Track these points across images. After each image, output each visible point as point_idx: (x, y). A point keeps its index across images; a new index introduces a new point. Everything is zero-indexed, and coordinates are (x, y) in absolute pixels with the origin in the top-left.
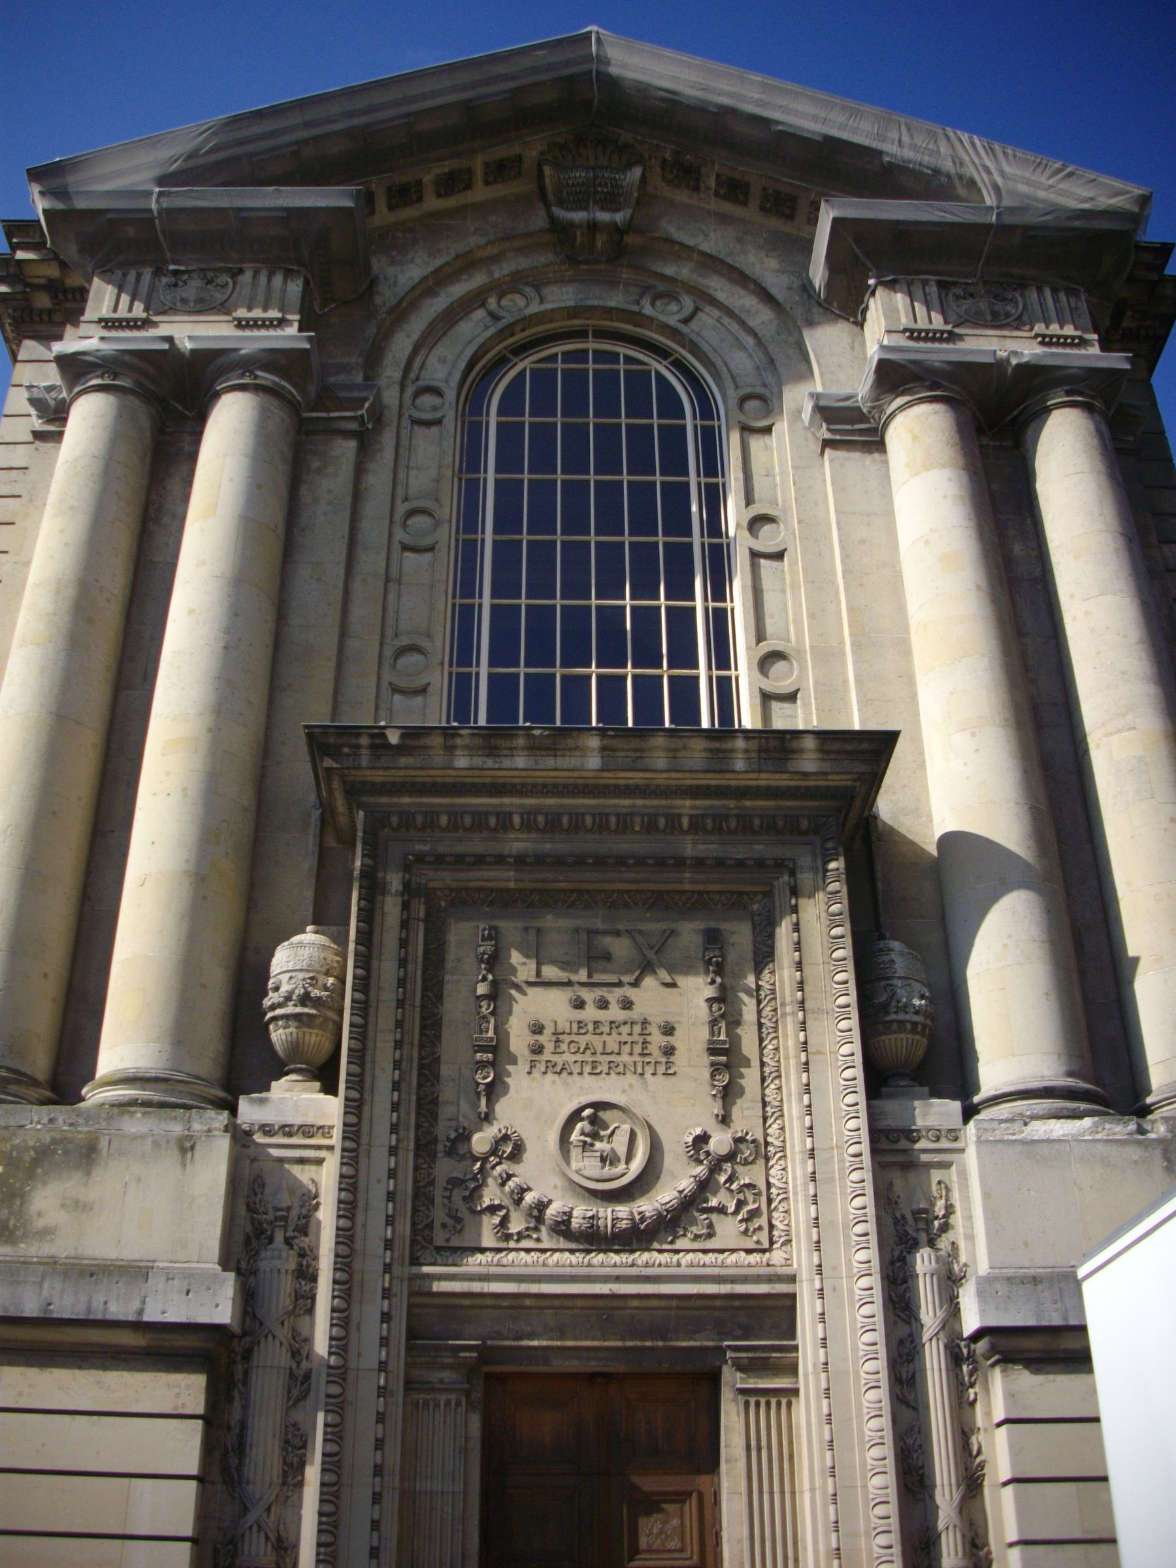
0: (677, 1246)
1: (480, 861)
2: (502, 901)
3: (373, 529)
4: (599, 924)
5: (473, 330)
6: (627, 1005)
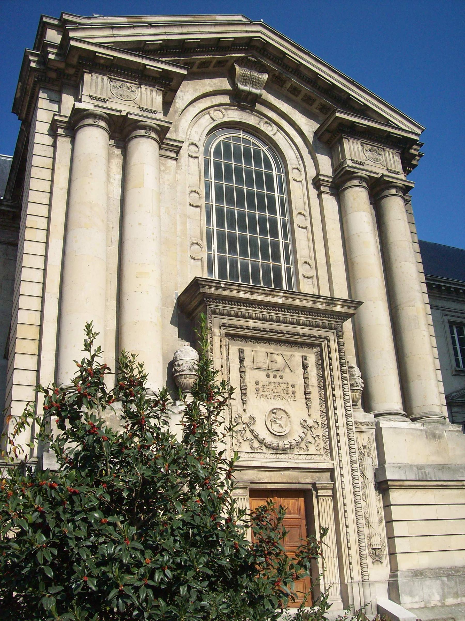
0: (301, 452)
1: (242, 327)
4: (273, 352)
5: (206, 123)
6: (281, 377)
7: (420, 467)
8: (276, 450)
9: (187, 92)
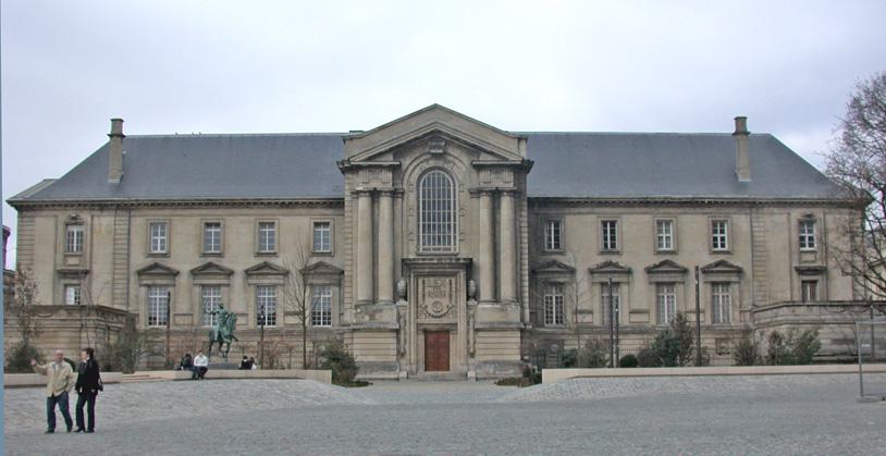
2: (425, 276)
3: (405, 213)
5: (418, 172)
7: (491, 323)
8: (435, 317)
9: (406, 162)
